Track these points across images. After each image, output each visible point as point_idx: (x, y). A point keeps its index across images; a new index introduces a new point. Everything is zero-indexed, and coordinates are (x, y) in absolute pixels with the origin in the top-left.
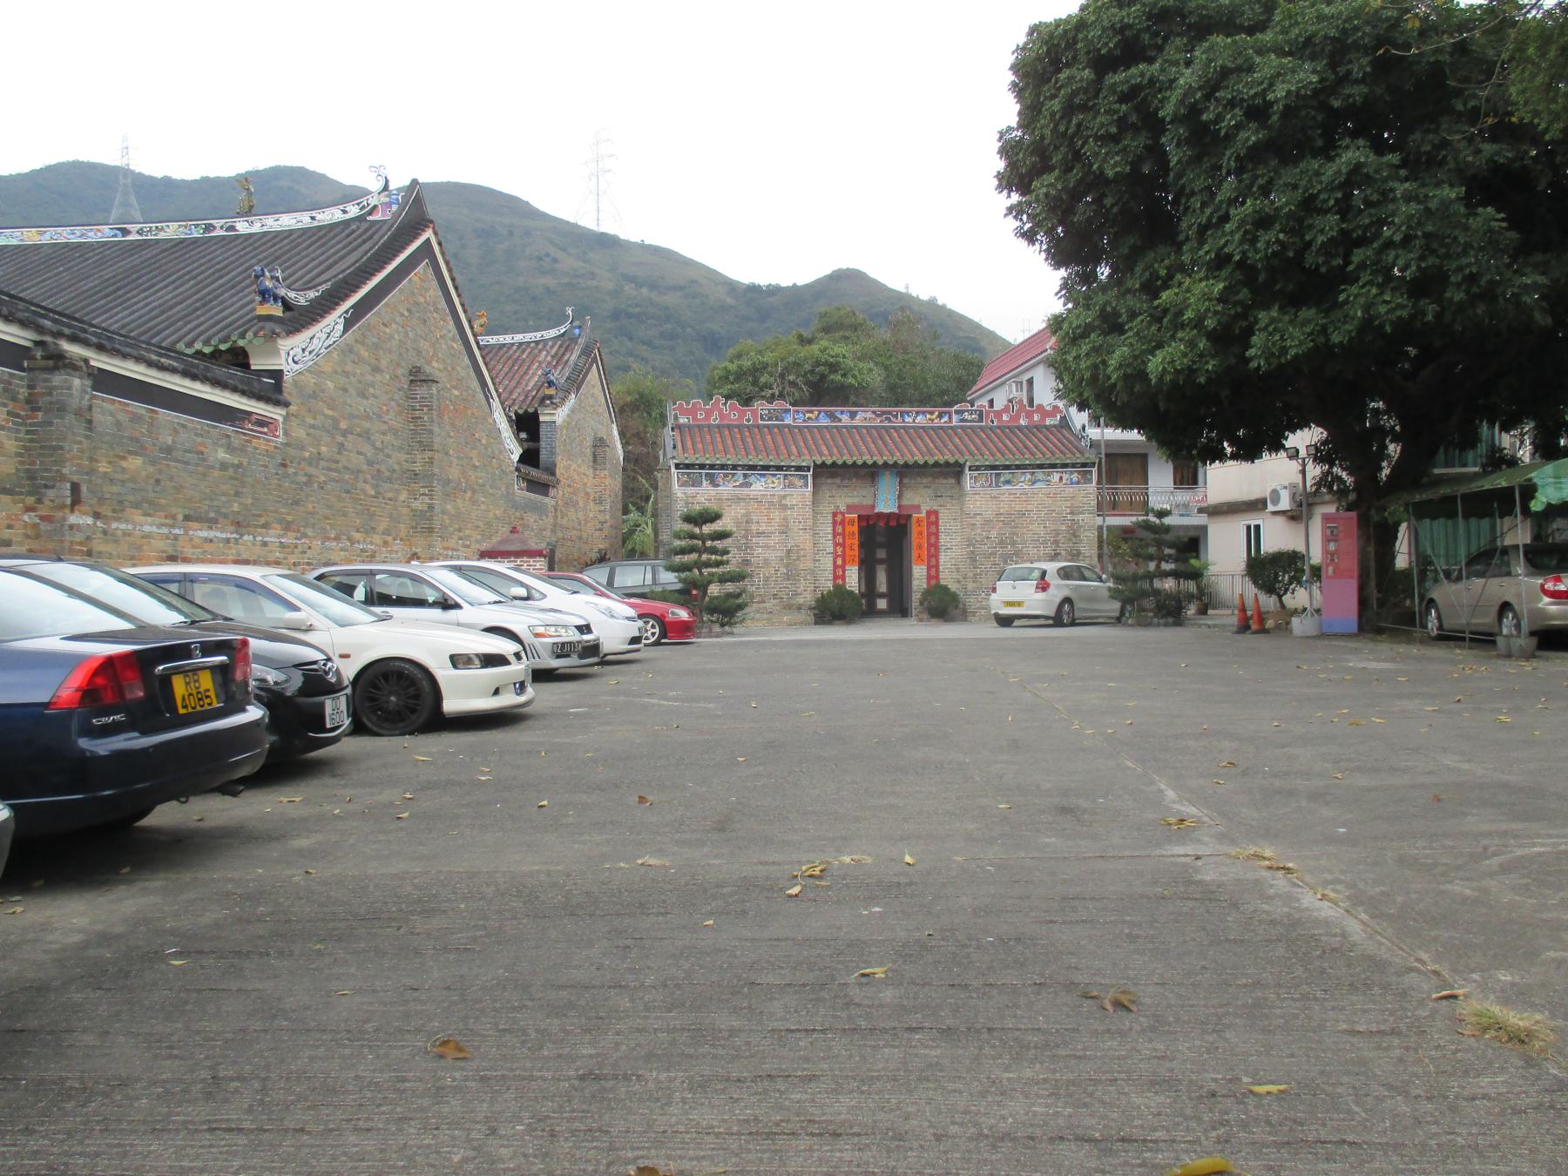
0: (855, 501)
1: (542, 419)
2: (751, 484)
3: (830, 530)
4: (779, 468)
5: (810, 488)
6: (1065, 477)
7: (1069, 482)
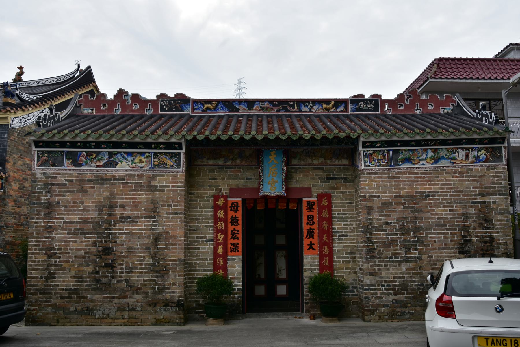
0: (240, 183)
2: (117, 164)
3: (210, 214)
4: (147, 145)
6: (472, 154)
7: (476, 160)
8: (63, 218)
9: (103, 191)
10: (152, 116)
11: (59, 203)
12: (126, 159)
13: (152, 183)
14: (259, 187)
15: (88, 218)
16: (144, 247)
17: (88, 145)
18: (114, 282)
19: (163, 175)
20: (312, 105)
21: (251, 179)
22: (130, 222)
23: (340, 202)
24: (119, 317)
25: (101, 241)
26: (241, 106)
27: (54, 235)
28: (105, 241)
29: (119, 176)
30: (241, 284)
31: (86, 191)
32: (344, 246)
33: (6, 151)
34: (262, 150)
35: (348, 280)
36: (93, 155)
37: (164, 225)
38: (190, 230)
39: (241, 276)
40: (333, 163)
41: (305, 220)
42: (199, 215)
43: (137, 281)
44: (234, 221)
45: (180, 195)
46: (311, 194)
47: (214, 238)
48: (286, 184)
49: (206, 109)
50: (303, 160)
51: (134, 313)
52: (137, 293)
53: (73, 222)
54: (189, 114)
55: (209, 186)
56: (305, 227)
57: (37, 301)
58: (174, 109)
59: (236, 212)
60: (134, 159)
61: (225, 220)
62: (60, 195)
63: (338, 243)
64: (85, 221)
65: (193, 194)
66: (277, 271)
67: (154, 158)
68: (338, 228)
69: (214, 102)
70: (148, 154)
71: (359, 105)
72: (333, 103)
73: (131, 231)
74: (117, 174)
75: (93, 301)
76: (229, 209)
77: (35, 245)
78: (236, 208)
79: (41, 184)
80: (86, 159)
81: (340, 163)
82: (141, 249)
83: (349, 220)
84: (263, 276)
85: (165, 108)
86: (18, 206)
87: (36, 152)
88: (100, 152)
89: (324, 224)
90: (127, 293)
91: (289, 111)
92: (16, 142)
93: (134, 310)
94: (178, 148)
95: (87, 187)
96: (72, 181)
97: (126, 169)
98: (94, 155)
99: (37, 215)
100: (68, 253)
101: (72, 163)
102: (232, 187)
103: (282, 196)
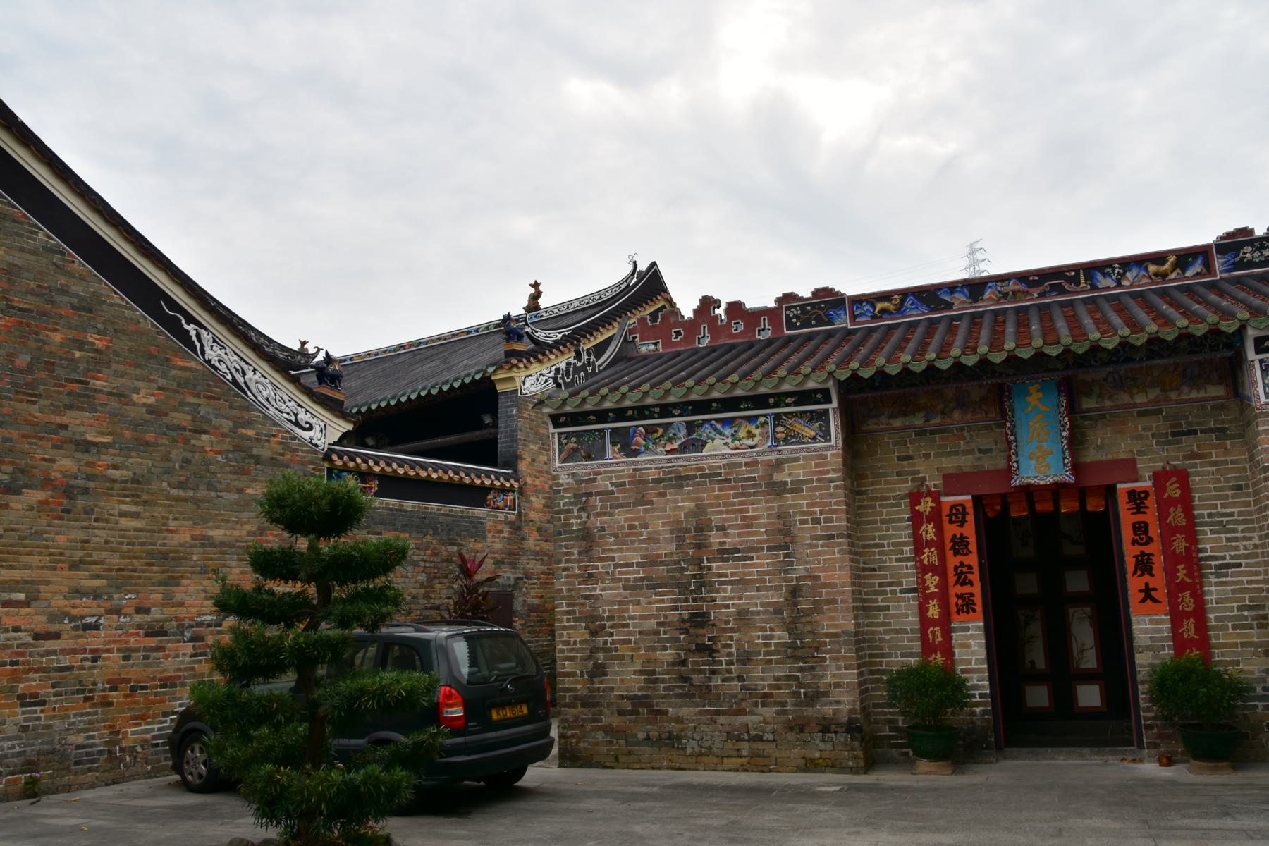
0: (965, 463)
1: (500, 388)
2: (704, 444)
3: (905, 534)
4: (760, 401)
5: (836, 438)
8: (612, 559)
9: (683, 501)
10: (769, 342)
11: (603, 529)
12: (720, 433)
13: (777, 477)
14: (1010, 467)
15: (659, 556)
16: (771, 609)
17: (647, 413)
18: (717, 681)
19: (797, 460)
20: (1121, 271)
21: (990, 451)
22: (738, 559)
23: (1212, 486)
24: (731, 753)
25: (686, 600)
26: (956, 295)
27: (598, 592)
28: (694, 600)
29: (710, 468)
30: (987, 683)
31: (650, 503)
32: (1233, 591)
33: (516, 440)
34: (1008, 386)
35: (1252, 673)
36: (657, 431)
37: (807, 563)
38: (864, 570)
39: (986, 666)
40: (1186, 397)
41: (1127, 534)
42: (881, 538)
43: (762, 679)
44: (960, 545)
45: (835, 497)
46: (1137, 472)
47: (918, 584)
48: (1072, 455)
49: (879, 312)
50: (1110, 398)
51: (760, 745)
52: (764, 705)
53: (632, 565)
54: (845, 328)
55: (899, 474)
56: (1130, 552)
57: (576, 718)
58: (813, 322)
59: (962, 526)
60: (735, 431)
61: (939, 545)
62: (604, 514)
63: (1217, 584)
64: (652, 561)
65: (865, 492)
66: (1075, 652)
67: (775, 426)
68: (1212, 549)
69: (896, 297)
70: (762, 419)
71: (1241, 255)
72: (1172, 259)
73: (742, 577)
74: (705, 464)
75: (679, 720)
76: (946, 519)
77: (567, 613)
78: (960, 516)
79: (568, 495)
80: (645, 441)
81: (1202, 394)
82: (765, 612)
83: (1240, 528)
84: (1041, 664)
85: (796, 323)
86: (544, 539)
87: (556, 436)
88: (671, 424)
89: (1175, 540)
90: (744, 704)
91: (1066, 292)
92: (533, 420)
93: (759, 738)
94: (822, 400)
95: (652, 494)
96: (623, 484)
97: (724, 452)
98: (661, 431)
99: (567, 554)
100: (627, 625)
101: (621, 450)
102: (947, 472)
103: (1065, 483)
